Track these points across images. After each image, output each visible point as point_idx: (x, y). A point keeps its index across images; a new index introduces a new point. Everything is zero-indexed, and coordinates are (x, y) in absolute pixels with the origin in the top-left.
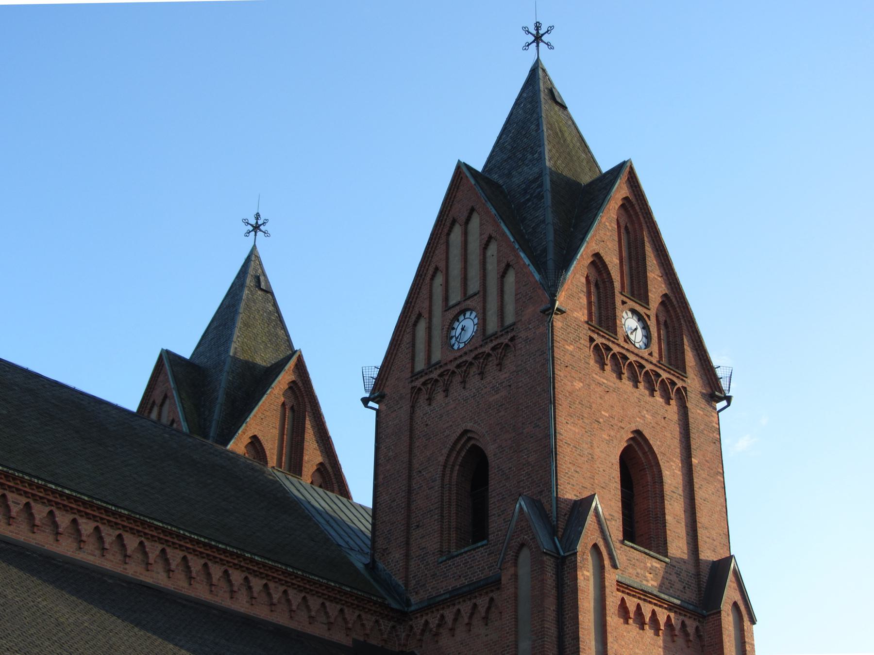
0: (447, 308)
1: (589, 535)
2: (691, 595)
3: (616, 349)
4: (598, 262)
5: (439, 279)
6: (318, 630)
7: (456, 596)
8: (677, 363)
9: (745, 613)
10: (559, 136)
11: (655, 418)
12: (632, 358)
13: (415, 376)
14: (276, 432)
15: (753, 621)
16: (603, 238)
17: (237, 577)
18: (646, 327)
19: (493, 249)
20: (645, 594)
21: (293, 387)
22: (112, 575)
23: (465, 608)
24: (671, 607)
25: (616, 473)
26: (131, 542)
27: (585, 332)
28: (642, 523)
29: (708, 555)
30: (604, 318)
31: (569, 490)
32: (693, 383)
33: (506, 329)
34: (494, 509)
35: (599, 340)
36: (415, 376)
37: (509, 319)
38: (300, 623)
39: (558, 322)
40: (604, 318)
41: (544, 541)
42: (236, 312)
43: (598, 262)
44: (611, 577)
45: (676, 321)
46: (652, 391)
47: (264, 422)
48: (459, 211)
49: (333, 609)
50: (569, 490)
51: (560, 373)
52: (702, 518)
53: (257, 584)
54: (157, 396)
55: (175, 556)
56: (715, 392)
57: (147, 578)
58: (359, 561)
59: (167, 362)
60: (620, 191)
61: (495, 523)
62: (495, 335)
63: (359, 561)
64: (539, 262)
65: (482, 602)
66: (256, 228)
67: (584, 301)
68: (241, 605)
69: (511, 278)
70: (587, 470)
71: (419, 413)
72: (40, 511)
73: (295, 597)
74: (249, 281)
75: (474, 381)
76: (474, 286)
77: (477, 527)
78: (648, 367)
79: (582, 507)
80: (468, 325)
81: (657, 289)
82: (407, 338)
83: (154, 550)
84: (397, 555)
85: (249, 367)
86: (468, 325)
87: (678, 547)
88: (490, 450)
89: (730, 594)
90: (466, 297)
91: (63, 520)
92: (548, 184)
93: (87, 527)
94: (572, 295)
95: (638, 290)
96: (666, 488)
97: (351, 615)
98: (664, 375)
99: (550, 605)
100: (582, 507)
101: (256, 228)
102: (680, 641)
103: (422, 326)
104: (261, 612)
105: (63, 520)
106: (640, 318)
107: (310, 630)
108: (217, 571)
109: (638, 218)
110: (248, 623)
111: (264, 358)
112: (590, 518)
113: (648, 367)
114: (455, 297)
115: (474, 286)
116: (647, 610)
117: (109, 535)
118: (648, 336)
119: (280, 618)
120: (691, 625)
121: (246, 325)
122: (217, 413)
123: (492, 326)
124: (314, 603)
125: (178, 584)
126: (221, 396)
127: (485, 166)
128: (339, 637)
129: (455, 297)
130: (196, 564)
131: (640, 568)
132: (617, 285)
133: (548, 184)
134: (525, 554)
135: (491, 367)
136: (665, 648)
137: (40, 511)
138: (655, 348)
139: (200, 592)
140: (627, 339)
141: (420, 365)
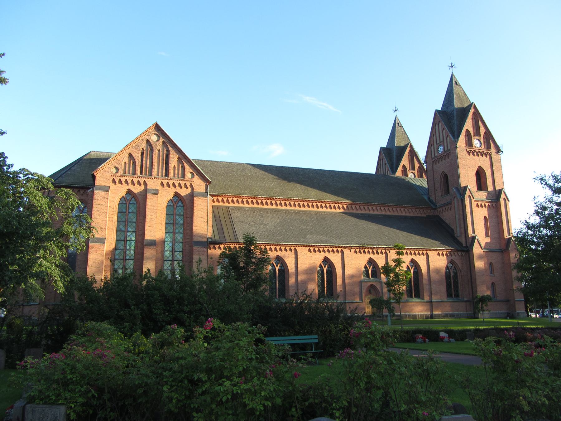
0: (437, 144)
1: (468, 193)
2: (494, 198)
3: (473, 150)
4: (467, 131)
5: (435, 137)
6: (419, 215)
7: (445, 205)
8: (489, 147)
9: (506, 200)
10: (459, 96)
11: (484, 162)
12: (477, 150)
13: (432, 158)
14: (408, 162)
15: (508, 201)
16: (469, 125)
17: (402, 209)
18: (480, 142)
19: (444, 131)
20: (482, 201)
21: (410, 151)
22: (380, 215)
23: (447, 207)
24: (489, 202)
25: (475, 177)
26: (382, 208)
27: (465, 149)
28: (481, 184)
29: (498, 188)
30: (469, 143)
31: (463, 185)
32: (493, 150)
33: (449, 150)
34: (450, 188)
35: (468, 150)
36: (432, 158)
37: (449, 148)
38: (416, 215)
39: (458, 149)
40: (469, 143)
41: (458, 196)
42: (395, 134)
43: (467, 131)
44: (473, 200)
45: (489, 137)
46: (482, 156)
47: (405, 161)
48: (437, 121)
49: (421, 211)
50: (463, 185)
51: (459, 160)
52: (496, 180)
53: (406, 210)
54: (381, 157)
55: (390, 209)
56: (498, 150)
57: (386, 214)
58: (426, 198)
59: (382, 149)
60: (472, 110)
61: (450, 191)
62: (446, 152)
63: (426, 198)
64: (453, 136)
65: (449, 206)
66: (396, 110)
67: (464, 142)
68: (404, 214)
69: (448, 138)
70: (467, 178)
71: (435, 166)
72: (366, 207)
73: (414, 210)
74: (397, 125)
75: (444, 161)
76: (442, 140)
77: (447, 191)
78: (481, 151)
79: (466, 188)
80: (441, 148)
81: (482, 130)
82: (430, 152)
83: (386, 209)
84: (433, 196)
85: (400, 147)
86: (441, 148)
87: (490, 188)
88: (448, 175)
89: (503, 196)
90: (440, 142)
91: (370, 208)
92: (455, 114)
93: (374, 208)
94: (461, 142)
95: (478, 133)
96: (487, 177)
97: (425, 211)
98: (485, 151)
99: (461, 209)
100: (466, 188)
101: (396, 110)
102: (492, 208)
103: (432, 147)
104: (408, 214)
105: (370, 208)
106: (479, 140)
107: (418, 215)
108: (398, 209)
109: (477, 116)
110: (406, 217)
111: (403, 144)
112: (468, 190)
113: (481, 151)
114: (438, 142)
115: (442, 140)
116: (483, 204)
117: (378, 208)
118: (481, 144)
119: (412, 215)
120: (494, 204)
121: (398, 137)
122: (394, 161)
123: (446, 149)
124: (418, 210)
125: (392, 213)
126: (395, 156)
127: (443, 106)
128: (423, 215)
129: (438, 142)
130: (394, 209)
131: (482, 195)
132: (472, 135)
133: (455, 114)
134: (455, 199)
135: (447, 158)
136: (488, 210)
137: (366, 207)
138: (483, 146)
139: (396, 214)
140: (475, 147)
141: (433, 157)
